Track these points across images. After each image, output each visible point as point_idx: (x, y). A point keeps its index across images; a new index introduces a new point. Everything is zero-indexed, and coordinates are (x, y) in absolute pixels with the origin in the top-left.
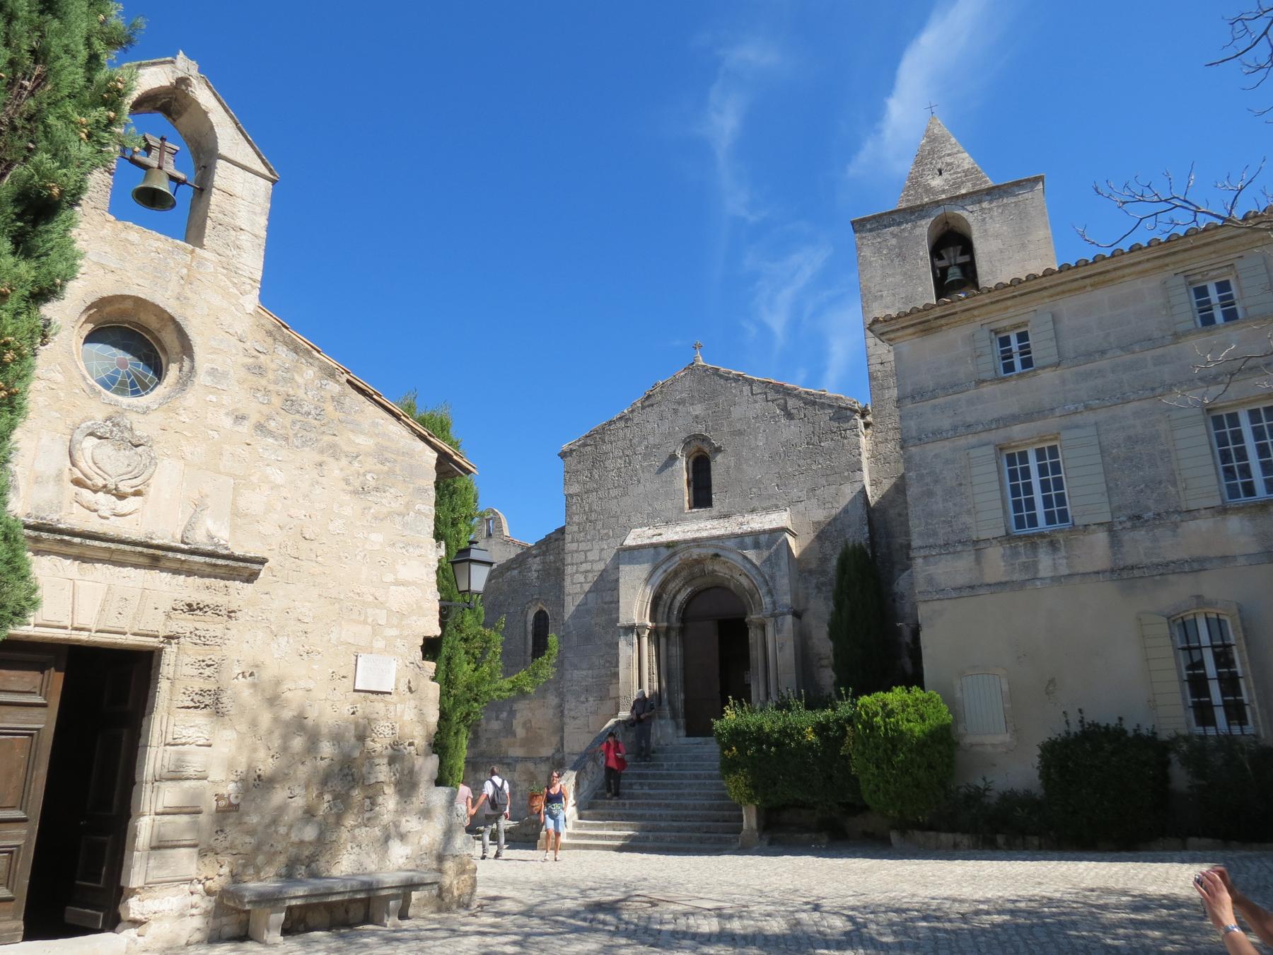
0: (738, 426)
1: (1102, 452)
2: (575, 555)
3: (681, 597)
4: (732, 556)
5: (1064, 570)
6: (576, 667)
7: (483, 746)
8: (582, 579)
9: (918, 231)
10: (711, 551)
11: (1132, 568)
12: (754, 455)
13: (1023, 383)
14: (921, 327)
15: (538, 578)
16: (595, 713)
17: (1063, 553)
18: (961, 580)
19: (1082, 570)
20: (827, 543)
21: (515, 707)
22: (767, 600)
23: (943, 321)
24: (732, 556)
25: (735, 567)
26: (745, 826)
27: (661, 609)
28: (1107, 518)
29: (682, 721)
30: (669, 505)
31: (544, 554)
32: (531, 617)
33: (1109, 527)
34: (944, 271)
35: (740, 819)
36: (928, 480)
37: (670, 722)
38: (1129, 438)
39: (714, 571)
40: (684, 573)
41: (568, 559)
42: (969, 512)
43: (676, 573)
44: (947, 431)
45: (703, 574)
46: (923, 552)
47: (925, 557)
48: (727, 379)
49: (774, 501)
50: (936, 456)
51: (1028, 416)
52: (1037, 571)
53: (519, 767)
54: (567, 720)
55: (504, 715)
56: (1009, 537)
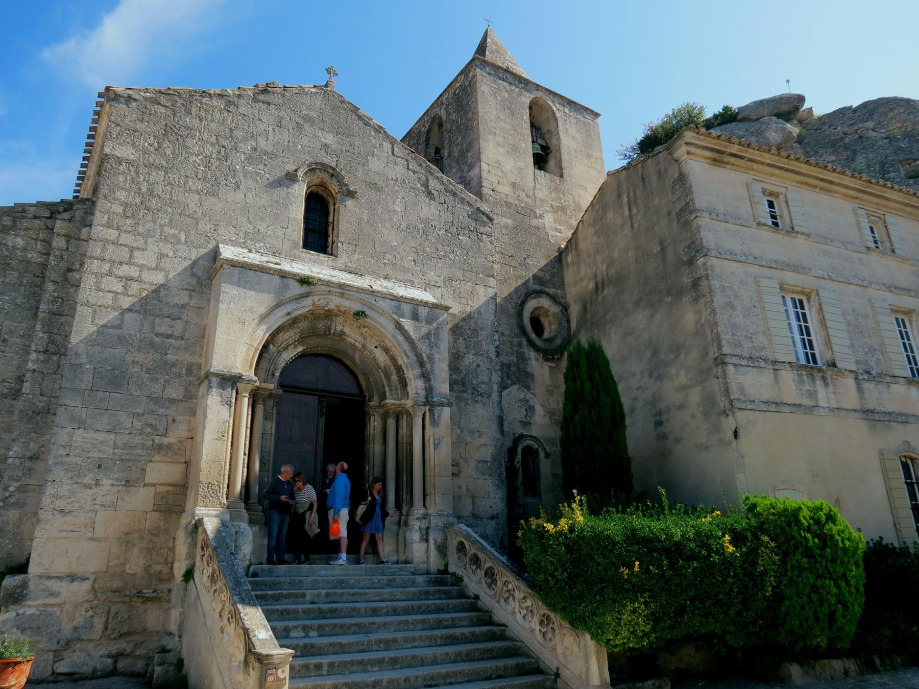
0: (376, 179)
2: (111, 248)
4: (381, 319)
6: (82, 425)
9: (523, 99)
10: (357, 307)
12: (391, 219)
13: (787, 239)
14: (716, 155)
20: (461, 340)
23: (732, 160)
24: (381, 319)
36: (729, 293)
39: (342, 333)
40: (303, 325)
41: (95, 249)
43: (295, 321)
45: (327, 332)
46: (735, 360)
47: (735, 365)
48: (367, 124)
49: (409, 276)
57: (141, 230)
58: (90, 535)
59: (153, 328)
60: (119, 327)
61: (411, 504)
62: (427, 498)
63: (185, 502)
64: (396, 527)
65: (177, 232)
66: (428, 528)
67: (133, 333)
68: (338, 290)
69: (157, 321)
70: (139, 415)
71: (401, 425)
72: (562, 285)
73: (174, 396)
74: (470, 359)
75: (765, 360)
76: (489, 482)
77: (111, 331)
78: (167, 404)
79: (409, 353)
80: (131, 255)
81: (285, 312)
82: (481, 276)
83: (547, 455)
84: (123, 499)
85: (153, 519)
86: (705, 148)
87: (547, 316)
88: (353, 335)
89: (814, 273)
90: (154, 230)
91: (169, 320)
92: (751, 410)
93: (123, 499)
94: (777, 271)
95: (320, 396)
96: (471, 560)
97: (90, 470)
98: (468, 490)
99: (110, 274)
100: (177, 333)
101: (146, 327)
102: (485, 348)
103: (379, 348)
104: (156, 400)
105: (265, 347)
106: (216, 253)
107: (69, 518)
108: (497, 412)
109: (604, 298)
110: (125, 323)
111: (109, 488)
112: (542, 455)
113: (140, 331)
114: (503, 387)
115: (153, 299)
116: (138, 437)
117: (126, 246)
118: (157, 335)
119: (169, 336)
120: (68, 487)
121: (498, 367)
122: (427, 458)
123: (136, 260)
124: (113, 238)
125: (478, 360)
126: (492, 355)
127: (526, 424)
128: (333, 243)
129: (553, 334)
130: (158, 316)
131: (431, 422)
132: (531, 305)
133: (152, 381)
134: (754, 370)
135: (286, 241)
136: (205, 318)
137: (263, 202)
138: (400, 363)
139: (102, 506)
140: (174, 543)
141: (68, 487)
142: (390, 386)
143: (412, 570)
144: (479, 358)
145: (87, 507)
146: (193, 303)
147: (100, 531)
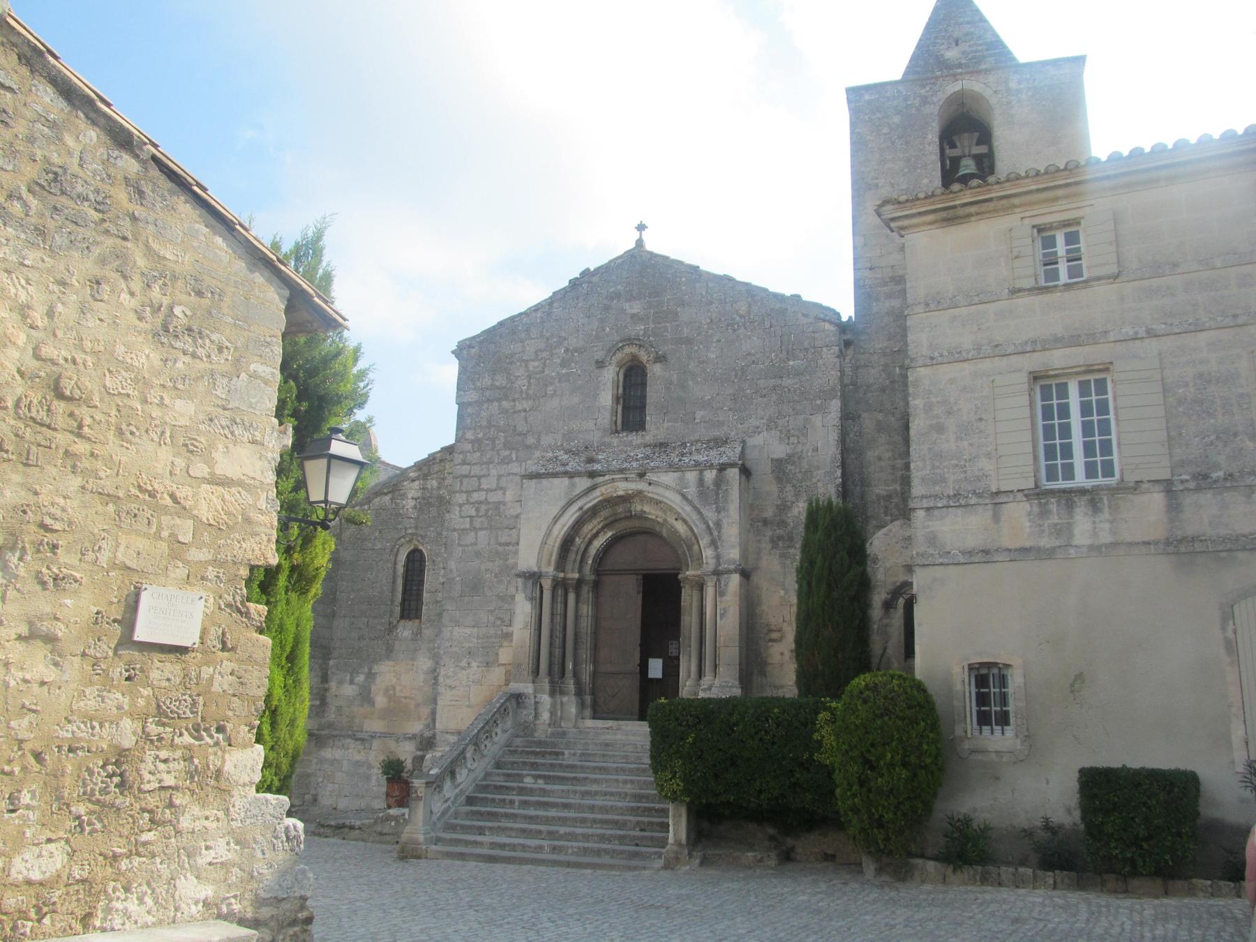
1: (1165, 390)
2: (466, 481)
3: (598, 543)
5: (1106, 538)
7: (331, 716)
8: (473, 513)
11: (1194, 539)
14: (944, 214)
15: (415, 507)
16: (479, 682)
17: (1106, 515)
18: (971, 543)
19: (1128, 539)
20: (789, 488)
21: (376, 669)
22: (708, 553)
23: (973, 209)
25: (671, 509)
26: (671, 840)
27: (572, 556)
28: (1166, 474)
29: (588, 699)
30: (591, 425)
31: (425, 477)
32: (402, 557)
33: (1168, 486)
34: (956, 162)
35: (665, 827)
37: (573, 698)
38: (1201, 375)
39: (643, 511)
40: (605, 513)
42: (988, 455)
43: (594, 511)
44: (968, 351)
45: (630, 517)
47: (928, 509)
50: (952, 381)
51: (1075, 341)
52: (1071, 535)
53: (376, 744)
54: (441, 689)
55: (361, 678)
56: (1037, 494)
60: (475, 544)
70: (492, 611)
75: (979, 495)
82: (819, 402)
86: (920, 214)
89: (1112, 337)
92: (941, 564)
94: (1036, 354)
99: (468, 502)
103: (680, 522)
107: (454, 692)
118: (500, 544)
119: (508, 544)
134: (959, 511)
137: (575, 400)
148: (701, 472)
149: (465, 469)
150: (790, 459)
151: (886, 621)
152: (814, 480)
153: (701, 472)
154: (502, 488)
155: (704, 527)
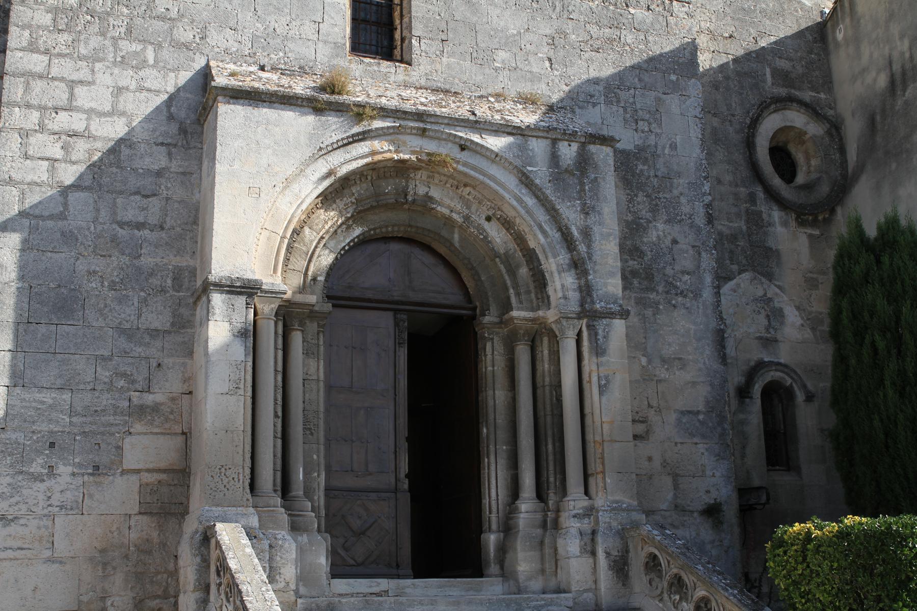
2: (38, 86)
4: (494, 170)
8: (58, 153)
20: (641, 197)
39: (428, 198)
57: (83, 51)
58: (48, 553)
59: (115, 213)
60: (62, 216)
61: (563, 491)
62: (592, 481)
63: (188, 498)
64: (539, 531)
65: (139, 47)
66: (594, 533)
67: (84, 224)
68: (416, 124)
69: (119, 201)
70: (103, 358)
71: (539, 356)
72: (827, 83)
73: (156, 325)
74: (659, 231)
76: (701, 447)
77: (50, 224)
78: (147, 339)
79: (547, 229)
80: (72, 94)
81: (324, 170)
82: (673, 77)
83: (810, 398)
84: (91, 496)
85: (142, 528)
87: (803, 143)
88: (447, 201)
90: (103, 48)
91: (138, 198)
93: (91, 496)
95: (396, 311)
96: (671, 585)
97: (39, 452)
98: (665, 464)
100: (153, 220)
101: (103, 213)
102: (686, 209)
104: (129, 334)
105: (297, 232)
106: (206, 74)
107: (13, 529)
108: (713, 324)
109: (906, 103)
110: (71, 209)
111: (69, 479)
112: (800, 396)
113: (95, 220)
114: (722, 278)
115: (111, 165)
116: (106, 395)
117: (62, 79)
118: (121, 225)
119: (140, 226)
120: (8, 479)
121: (711, 242)
122: (587, 410)
123: (79, 103)
124: (39, 69)
125: (675, 231)
126: (700, 221)
127: (768, 342)
128: (403, 40)
129: (814, 176)
130: (121, 193)
131: (591, 348)
132: (770, 124)
133: (120, 302)
135: (320, 45)
136: (196, 191)
138: (532, 244)
139: (61, 507)
140: (176, 563)
141: (8, 479)
142: (516, 286)
143: (571, 604)
144: (677, 228)
145: (39, 510)
146: (175, 166)
147: (62, 547)
148: (554, 142)
149: (37, 63)
150: (642, 153)
151: (741, 416)
152: (676, 192)
153: (554, 142)
154: (123, 114)
155: (558, 235)
